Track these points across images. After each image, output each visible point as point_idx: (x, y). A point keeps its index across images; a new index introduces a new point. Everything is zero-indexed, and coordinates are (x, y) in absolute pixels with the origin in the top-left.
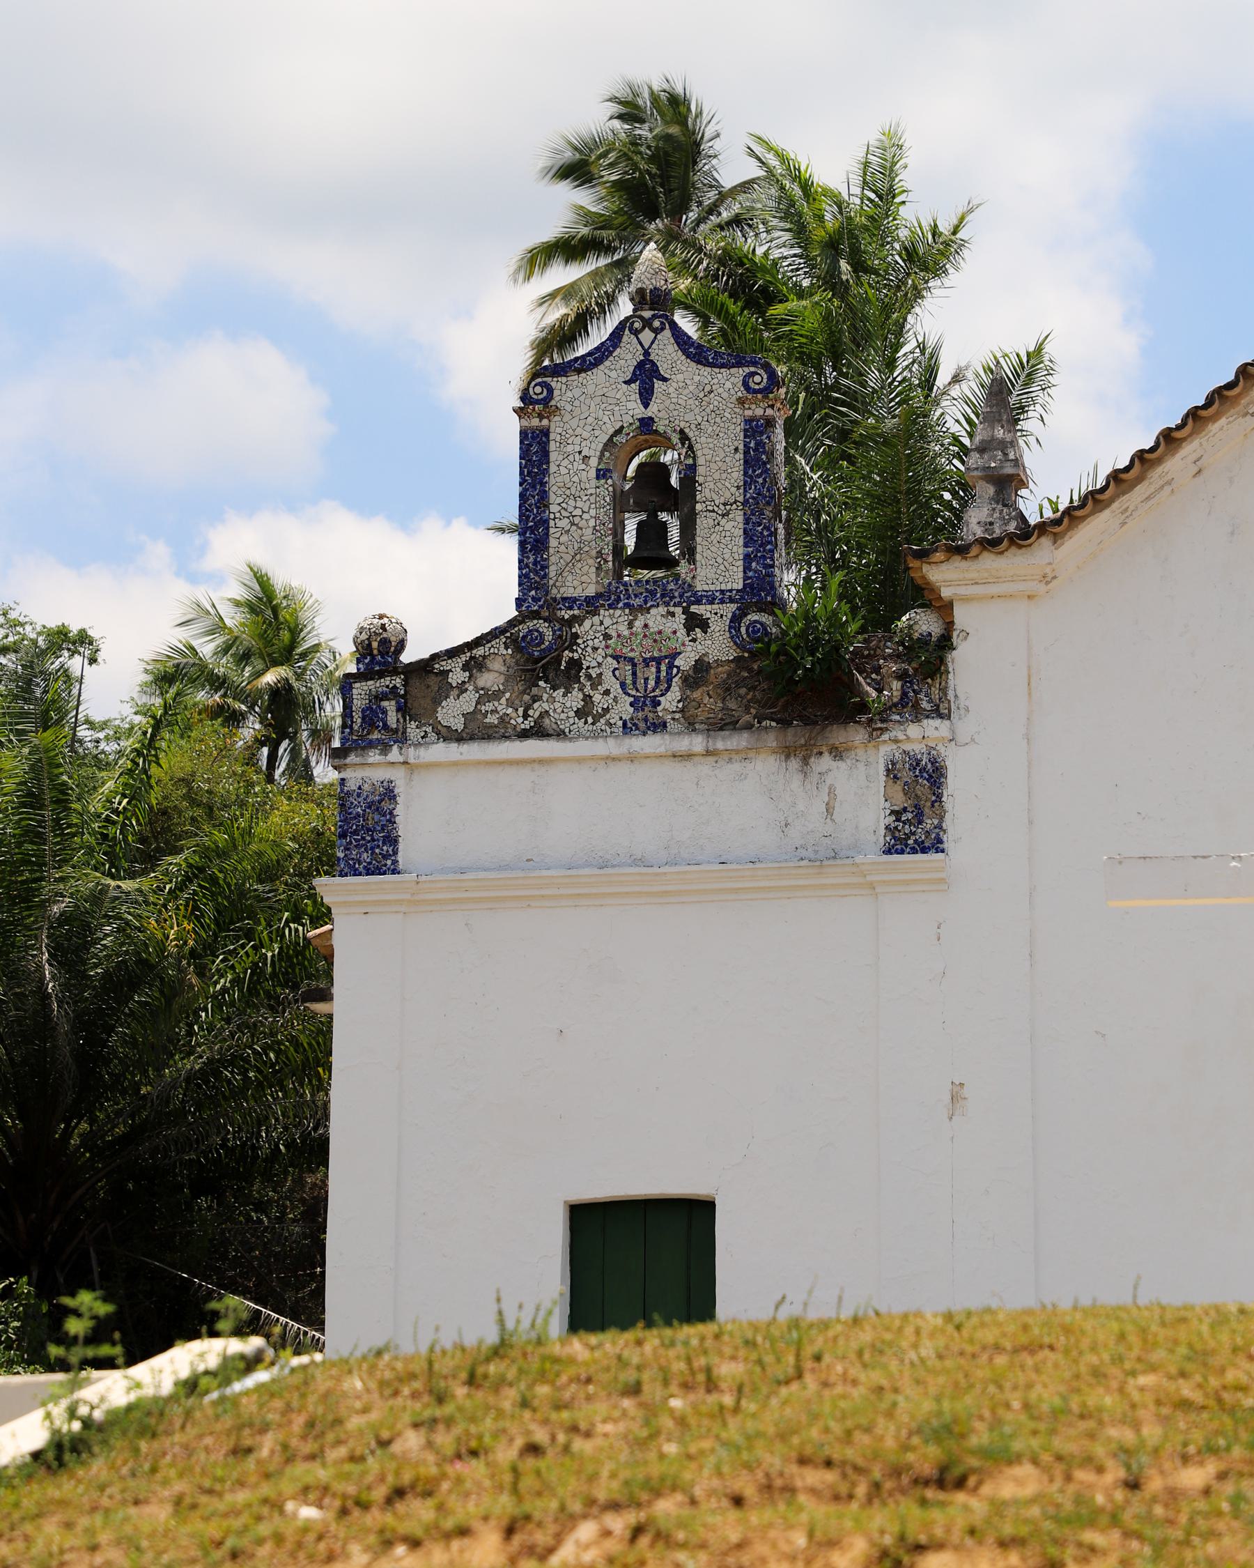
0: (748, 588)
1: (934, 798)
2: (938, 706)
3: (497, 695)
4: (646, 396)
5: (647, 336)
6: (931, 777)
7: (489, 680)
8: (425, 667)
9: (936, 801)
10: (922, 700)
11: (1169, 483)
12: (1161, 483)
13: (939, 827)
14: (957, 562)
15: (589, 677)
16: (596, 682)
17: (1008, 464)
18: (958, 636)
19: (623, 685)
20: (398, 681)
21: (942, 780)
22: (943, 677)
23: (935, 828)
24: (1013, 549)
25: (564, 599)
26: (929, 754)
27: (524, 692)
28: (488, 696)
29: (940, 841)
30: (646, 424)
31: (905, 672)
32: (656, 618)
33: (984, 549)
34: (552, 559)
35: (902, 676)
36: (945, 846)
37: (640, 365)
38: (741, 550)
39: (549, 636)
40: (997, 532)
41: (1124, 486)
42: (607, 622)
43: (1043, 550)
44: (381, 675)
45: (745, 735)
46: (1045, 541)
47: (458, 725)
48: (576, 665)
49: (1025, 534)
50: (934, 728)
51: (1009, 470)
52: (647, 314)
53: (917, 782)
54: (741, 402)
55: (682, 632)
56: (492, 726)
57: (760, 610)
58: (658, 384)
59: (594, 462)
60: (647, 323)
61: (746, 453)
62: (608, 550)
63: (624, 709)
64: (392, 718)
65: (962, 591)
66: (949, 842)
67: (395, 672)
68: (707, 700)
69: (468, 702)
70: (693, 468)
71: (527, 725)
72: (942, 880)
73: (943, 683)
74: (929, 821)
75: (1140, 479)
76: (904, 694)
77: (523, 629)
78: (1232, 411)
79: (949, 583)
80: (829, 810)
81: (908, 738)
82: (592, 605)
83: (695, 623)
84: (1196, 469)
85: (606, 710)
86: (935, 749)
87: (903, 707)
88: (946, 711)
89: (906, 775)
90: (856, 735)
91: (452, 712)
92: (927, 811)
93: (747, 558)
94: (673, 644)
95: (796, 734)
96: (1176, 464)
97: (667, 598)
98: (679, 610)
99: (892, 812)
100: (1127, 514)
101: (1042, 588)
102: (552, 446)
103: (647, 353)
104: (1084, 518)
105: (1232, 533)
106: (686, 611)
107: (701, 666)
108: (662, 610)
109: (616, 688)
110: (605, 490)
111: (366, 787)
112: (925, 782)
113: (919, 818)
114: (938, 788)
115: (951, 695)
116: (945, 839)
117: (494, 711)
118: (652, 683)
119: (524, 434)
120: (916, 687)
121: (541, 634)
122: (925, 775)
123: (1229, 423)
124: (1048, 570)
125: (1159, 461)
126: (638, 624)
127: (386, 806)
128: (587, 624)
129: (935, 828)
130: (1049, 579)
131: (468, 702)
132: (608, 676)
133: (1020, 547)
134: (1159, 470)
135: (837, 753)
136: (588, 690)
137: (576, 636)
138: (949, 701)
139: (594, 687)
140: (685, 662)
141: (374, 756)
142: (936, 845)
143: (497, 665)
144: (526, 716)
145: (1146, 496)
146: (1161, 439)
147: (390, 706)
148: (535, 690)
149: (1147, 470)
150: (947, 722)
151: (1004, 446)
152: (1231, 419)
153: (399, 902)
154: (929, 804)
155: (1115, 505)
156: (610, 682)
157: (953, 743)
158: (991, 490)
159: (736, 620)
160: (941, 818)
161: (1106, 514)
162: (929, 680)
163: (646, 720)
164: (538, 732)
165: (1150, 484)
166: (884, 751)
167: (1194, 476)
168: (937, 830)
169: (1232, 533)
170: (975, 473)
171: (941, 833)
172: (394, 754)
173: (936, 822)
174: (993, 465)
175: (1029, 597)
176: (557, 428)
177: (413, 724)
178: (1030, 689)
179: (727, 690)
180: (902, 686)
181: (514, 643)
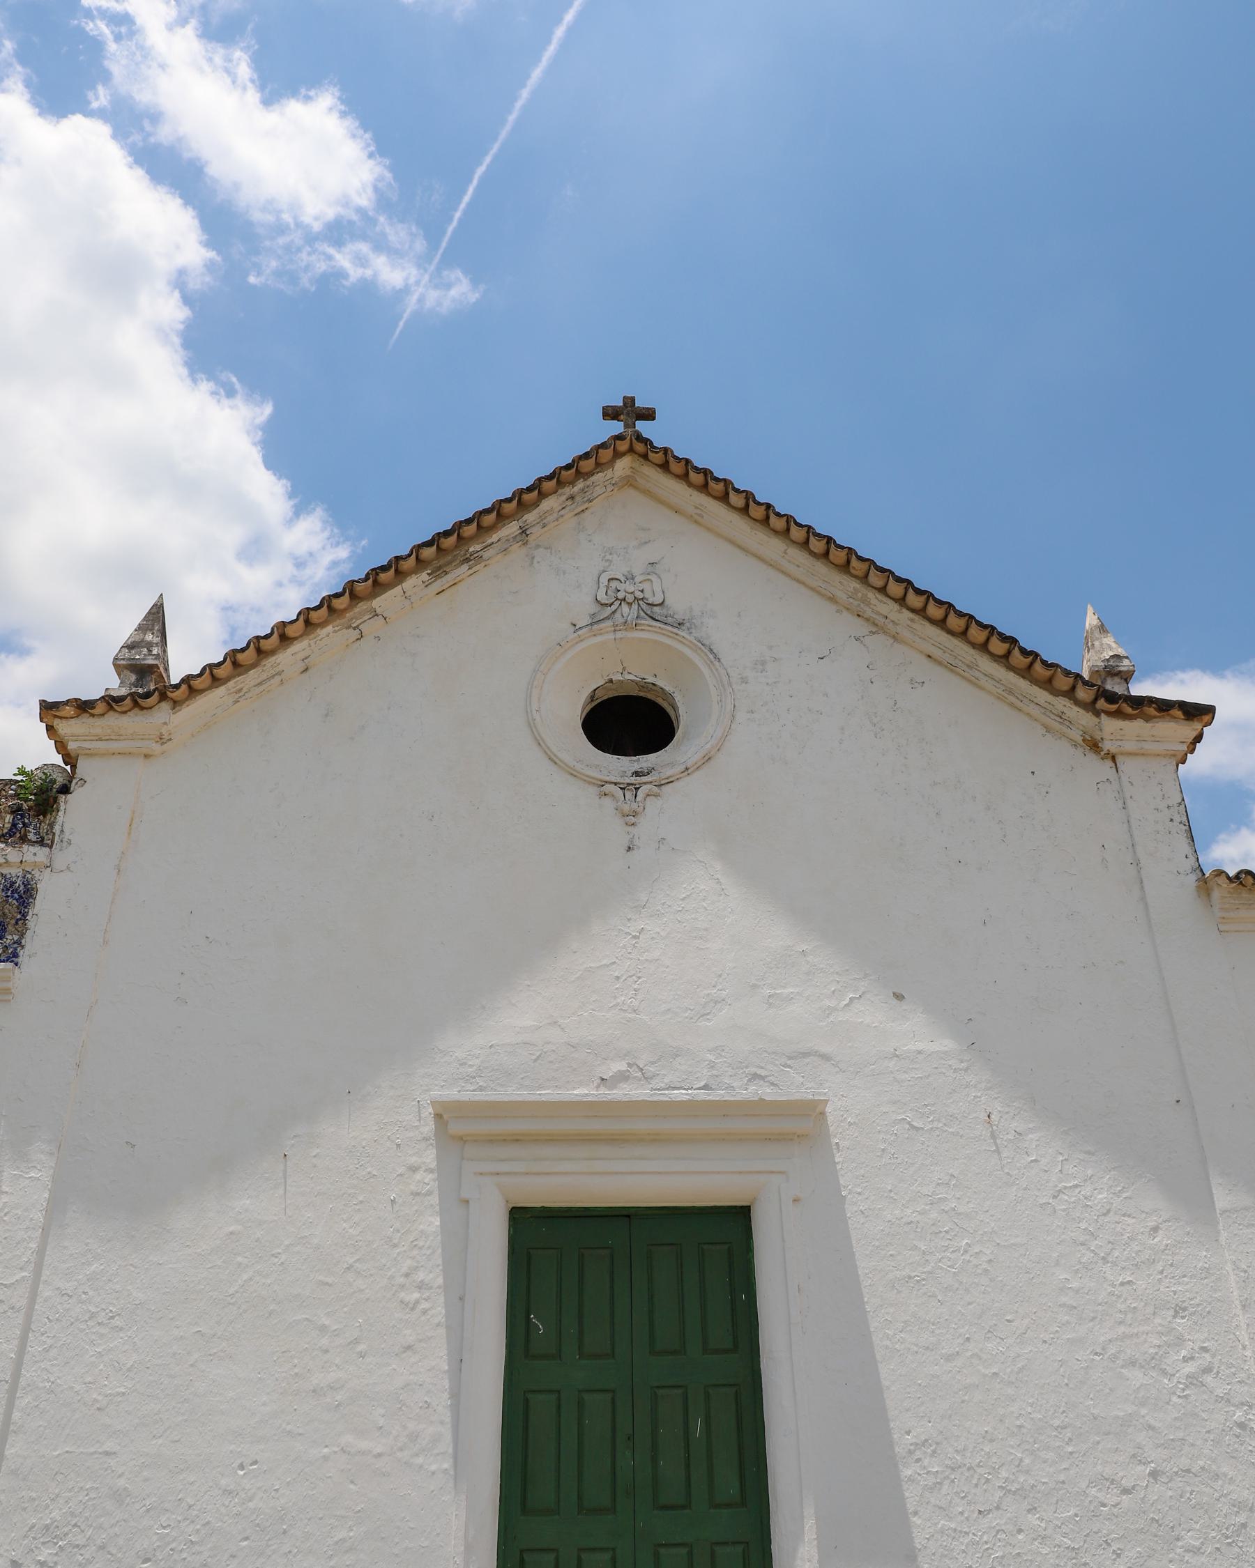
1: (19, 916)
2: (43, 839)
6: (21, 897)
9: (20, 919)
10: (30, 832)
11: (279, 673)
12: (273, 672)
13: (19, 943)
14: (85, 718)
17: (151, 657)
18: (77, 783)
21: (31, 900)
22: (54, 813)
23: (14, 943)
24: (136, 710)
26: (24, 877)
29: (15, 955)
31: (20, 808)
33: (111, 708)
35: (16, 811)
36: (19, 960)
41: (240, 670)
46: (165, 706)
51: (150, 661)
53: (7, 901)
65: (86, 745)
66: (23, 956)
73: (52, 819)
74: (10, 937)
75: (254, 666)
76: (14, 825)
78: (338, 621)
81: (7, 862)
84: (301, 666)
86: (30, 873)
87: (11, 836)
88: (49, 842)
92: (10, 928)
96: (287, 658)
100: (241, 694)
101: (157, 748)
104: (202, 691)
105: (327, 715)
112: (15, 902)
114: (26, 907)
115: (57, 829)
116: (21, 953)
120: (26, 821)
122: (16, 896)
123: (335, 632)
124: (164, 731)
125: (272, 652)
129: (14, 943)
130: (164, 741)
133: (142, 708)
134: (272, 660)
138: (54, 834)
145: (259, 680)
146: (275, 629)
149: (262, 659)
150: (46, 850)
151: (149, 645)
152: (337, 629)
154: (13, 922)
155: (231, 684)
157: (49, 869)
160: (22, 935)
161: (221, 690)
162: (41, 817)
165: (263, 671)
167: (302, 672)
168: (16, 945)
169: (327, 715)
170: (122, 662)
171: (19, 949)
173: (16, 938)
174: (138, 657)
175: (146, 756)
178: (130, 829)
180: (13, 819)
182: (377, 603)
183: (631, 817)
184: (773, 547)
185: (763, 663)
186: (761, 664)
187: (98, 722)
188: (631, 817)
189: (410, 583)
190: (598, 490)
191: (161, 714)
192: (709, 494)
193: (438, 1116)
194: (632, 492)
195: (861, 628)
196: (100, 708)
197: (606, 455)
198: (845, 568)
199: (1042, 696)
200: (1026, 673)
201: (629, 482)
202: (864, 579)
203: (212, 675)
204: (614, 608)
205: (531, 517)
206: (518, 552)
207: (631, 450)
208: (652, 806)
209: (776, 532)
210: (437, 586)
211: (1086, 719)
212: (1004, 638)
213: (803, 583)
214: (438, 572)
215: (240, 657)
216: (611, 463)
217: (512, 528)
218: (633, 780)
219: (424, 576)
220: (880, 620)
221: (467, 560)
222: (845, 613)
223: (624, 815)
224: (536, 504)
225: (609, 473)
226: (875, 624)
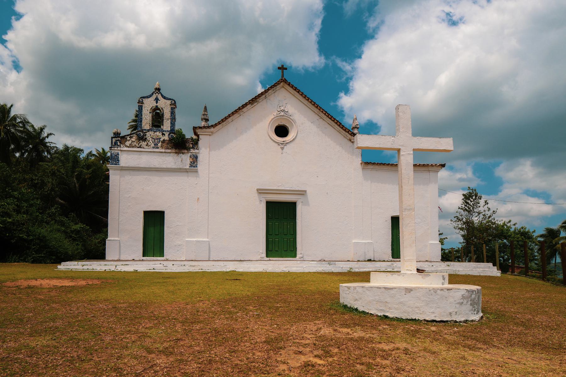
0: (171, 130)
3: (134, 142)
4: (157, 102)
5: (157, 94)
7: (133, 140)
8: (123, 137)
13: (197, 164)
15: (148, 140)
16: (149, 141)
19: (153, 142)
20: (119, 139)
25: (144, 129)
27: (138, 142)
28: (133, 142)
30: (157, 106)
32: (158, 133)
33: (204, 128)
34: (143, 124)
35: (192, 144)
37: (156, 98)
38: (170, 125)
39: (142, 134)
40: (205, 126)
42: (151, 133)
43: (212, 129)
44: (117, 138)
45: (170, 150)
46: (212, 128)
47: (129, 145)
48: (146, 138)
49: (209, 127)
50: (196, 151)
52: (157, 91)
54: (170, 105)
55: (161, 135)
56: (133, 146)
57: (173, 133)
58: (158, 101)
59: (149, 111)
60: (157, 92)
61: (171, 112)
62: (151, 123)
63: (153, 145)
64: (119, 144)
67: (119, 137)
68: (165, 145)
69: (130, 142)
70: (163, 113)
71: (139, 146)
72: (197, 171)
75: (225, 121)
76: (193, 146)
77: (138, 133)
79: (199, 132)
80: (182, 161)
82: (148, 131)
83: (163, 134)
85: (150, 145)
89: (192, 157)
90: (186, 151)
91: (128, 143)
93: (171, 126)
94: (160, 137)
96: (230, 119)
97: (159, 130)
98: (161, 132)
99: (191, 162)
101: (211, 134)
102: (143, 108)
103: (157, 97)
104: (217, 125)
105: (236, 129)
106: (162, 132)
107: (164, 140)
108: (159, 132)
109: (152, 142)
110: (151, 115)
111: (115, 153)
113: (194, 163)
117: (134, 144)
118: (157, 142)
119: (139, 106)
121: (141, 134)
126: (155, 134)
127: (118, 156)
128: (148, 133)
131: (130, 142)
132: (150, 140)
133: (209, 128)
134: (227, 120)
135: (183, 153)
136: (148, 142)
137: (146, 135)
139: (148, 142)
140: (162, 140)
141: (116, 149)
142: (197, 167)
143: (134, 138)
144: (138, 145)
147: (118, 142)
148: (140, 142)
151: (206, 115)
153: (119, 169)
156: (151, 141)
158: (205, 121)
159: (169, 134)
163: (156, 147)
164: (140, 147)
166: (189, 154)
169: (236, 129)
172: (119, 149)
176: (144, 105)
177: (122, 145)
179: (168, 144)
181: (137, 135)
182: (243, 110)
183: (282, 148)
184: (306, 102)
185: (303, 123)
186: (302, 124)
187: (203, 130)
188: (282, 148)
189: (248, 106)
190: (278, 89)
192: (296, 91)
193: (257, 190)
194: (283, 88)
195: (318, 118)
196: (203, 128)
197: (279, 83)
198: (317, 107)
199: (344, 132)
200: (342, 128)
201: (283, 87)
202: (320, 110)
204: (280, 112)
205: (267, 94)
206: (265, 101)
207: (283, 81)
208: (285, 147)
209: (307, 100)
210: (252, 107)
211: (350, 136)
212: (340, 123)
213: (310, 109)
214: (252, 104)
215: (223, 120)
216: (280, 83)
217: (264, 96)
218: (283, 142)
219: (250, 105)
220: (321, 116)
221: (257, 102)
222: (316, 115)
223: (281, 148)
224: (268, 92)
225: (280, 85)
226: (321, 117)
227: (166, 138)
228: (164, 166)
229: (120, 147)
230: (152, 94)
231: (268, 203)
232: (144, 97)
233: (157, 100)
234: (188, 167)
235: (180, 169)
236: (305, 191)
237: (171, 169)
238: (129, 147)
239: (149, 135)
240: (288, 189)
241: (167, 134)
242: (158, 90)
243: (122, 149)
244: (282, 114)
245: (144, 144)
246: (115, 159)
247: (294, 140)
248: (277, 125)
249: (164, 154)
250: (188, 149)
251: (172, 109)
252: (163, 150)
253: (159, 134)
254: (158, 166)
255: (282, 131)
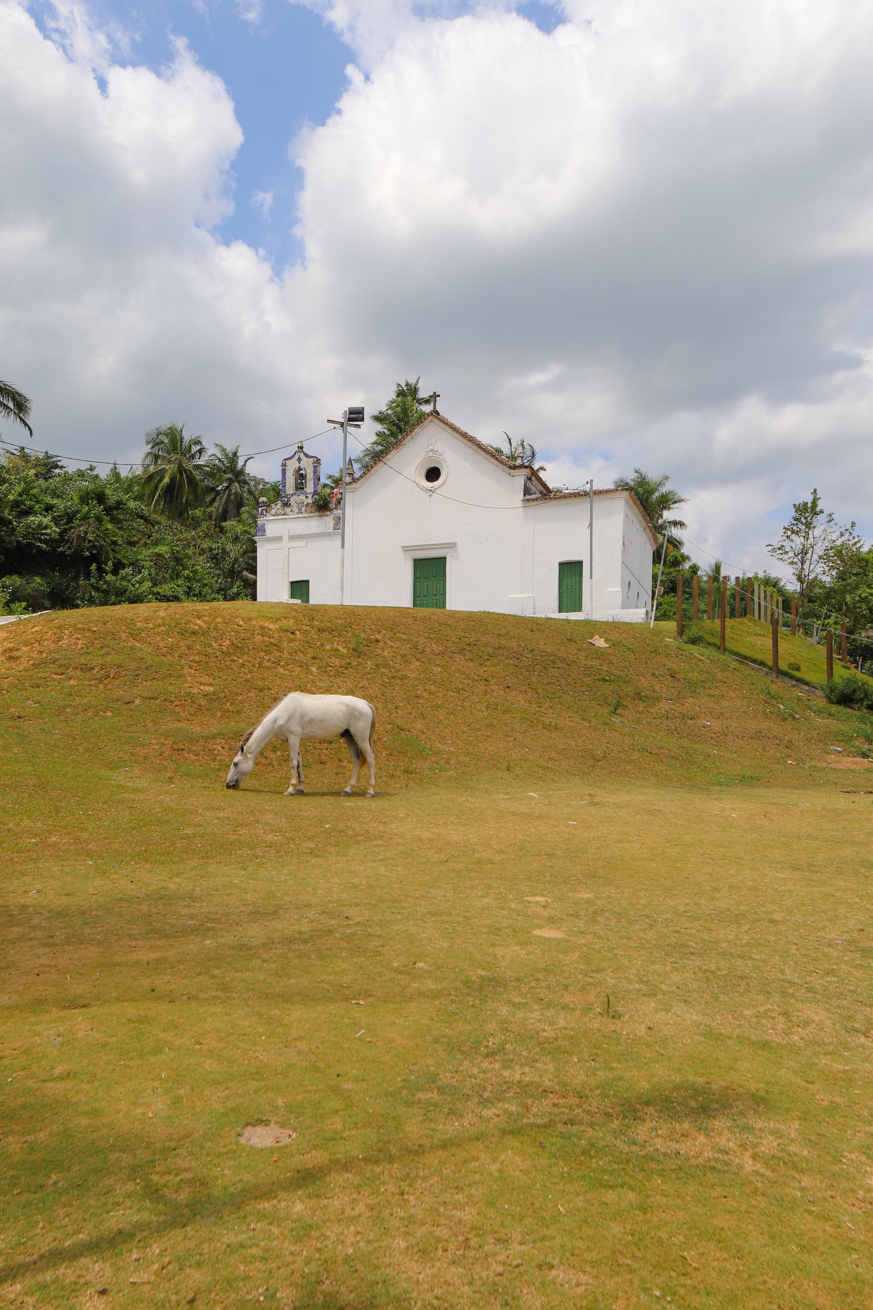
4: (299, 463)
7: (278, 507)
28: (278, 509)
63: (297, 511)
68: (308, 508)
82: (292, 495)
83: (307, 497)
90: (329, 513)
91: (273, 512)
95: (320, 513)
107: (308, 504)
135: (326, 515)
140: (305, 503)
166: (332, 517)
188: (431, 496)
191: (354, 485)
203: (361, 477)
227: (310, 500)
228: (308, 532)
229: (266, 516)
230: (295, 454)
231: (415, 560)
232: (286, 459)
233: (299, 459)
234: (331, 530)
235: (324, 533)
236: (455, 544)
237: (315, 534)
238: (274, 516)
239: (293, 500)
240: (434, 543)
241: (310, 496)
242: (301, 448)
243: (267, 518)
244: (431, 454)
245: (288, 510)
246: (263, 531)
247: (443, 483)
248: (427, 467)
249: (308, 519)
250: (331, 510)
251: (315, 467)
252: (307, 515)
253: (302, 497)
254: (302, 533)
255: (433, 474)
